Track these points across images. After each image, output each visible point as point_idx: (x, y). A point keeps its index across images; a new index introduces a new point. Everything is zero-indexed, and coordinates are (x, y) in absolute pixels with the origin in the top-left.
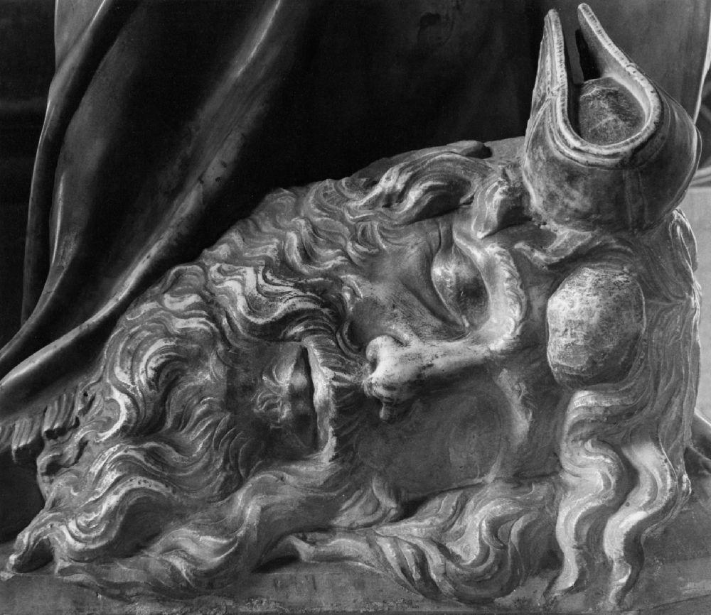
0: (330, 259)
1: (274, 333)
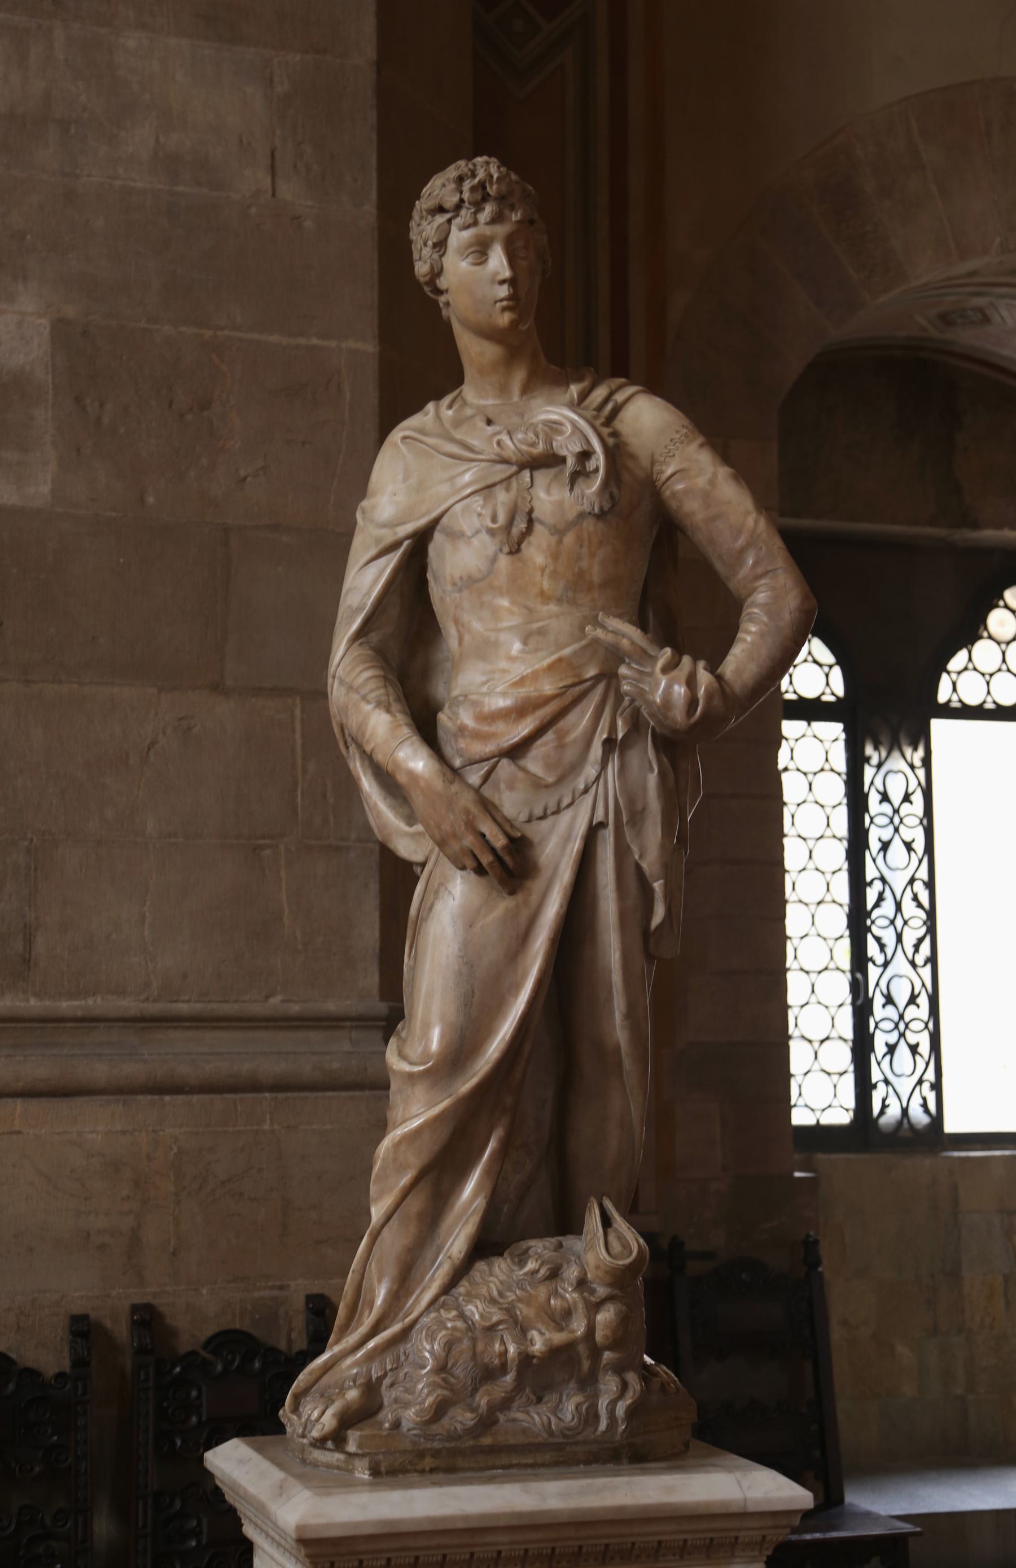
0: (511, 1296)
1: (492, 1328)
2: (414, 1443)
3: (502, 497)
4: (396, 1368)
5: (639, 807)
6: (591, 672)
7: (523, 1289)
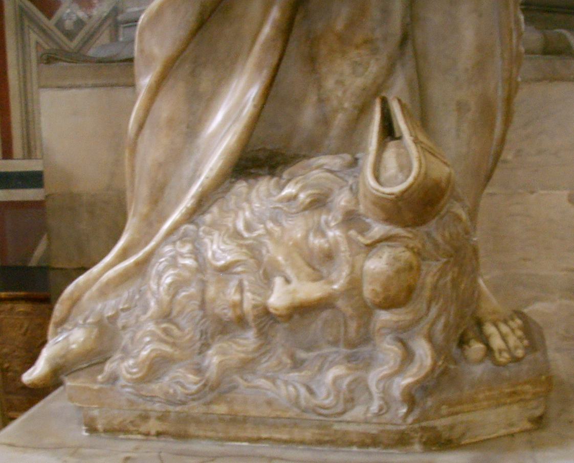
1: (226, 269)
2: (131, 403)
7: (276, 221)
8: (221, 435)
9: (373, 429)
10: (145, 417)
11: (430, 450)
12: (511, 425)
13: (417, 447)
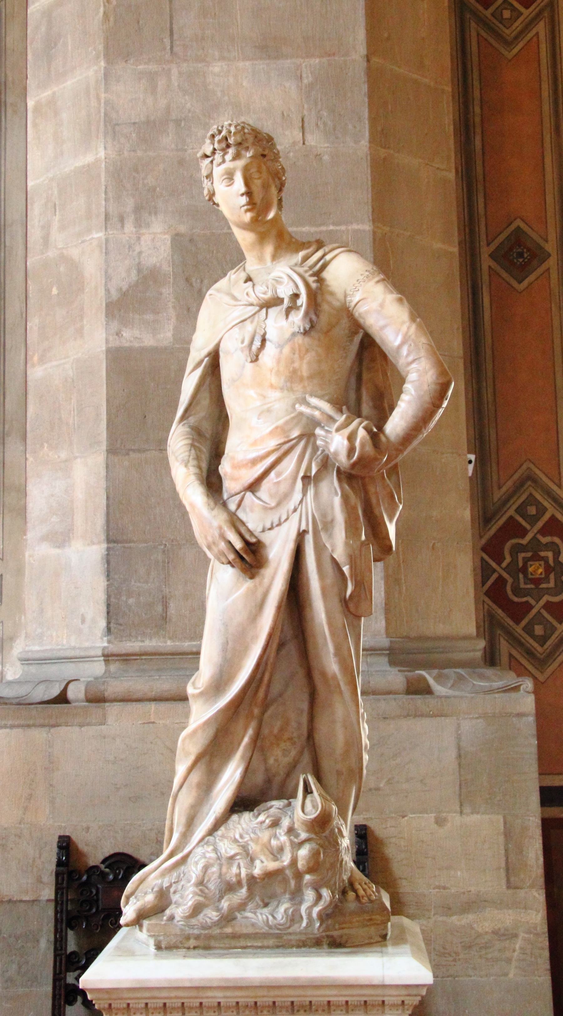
0: (247, 838)
2: (182, 930)
3: (249, 327)
4: (177, 882)
5: (329, 518)
6: (295, 433)
7: (254, 833)
8: (227, 946)
9: (303, 938)
10: (188, 938)
11: (331, 948)
12: (371, 938)
13: (325, 946)
